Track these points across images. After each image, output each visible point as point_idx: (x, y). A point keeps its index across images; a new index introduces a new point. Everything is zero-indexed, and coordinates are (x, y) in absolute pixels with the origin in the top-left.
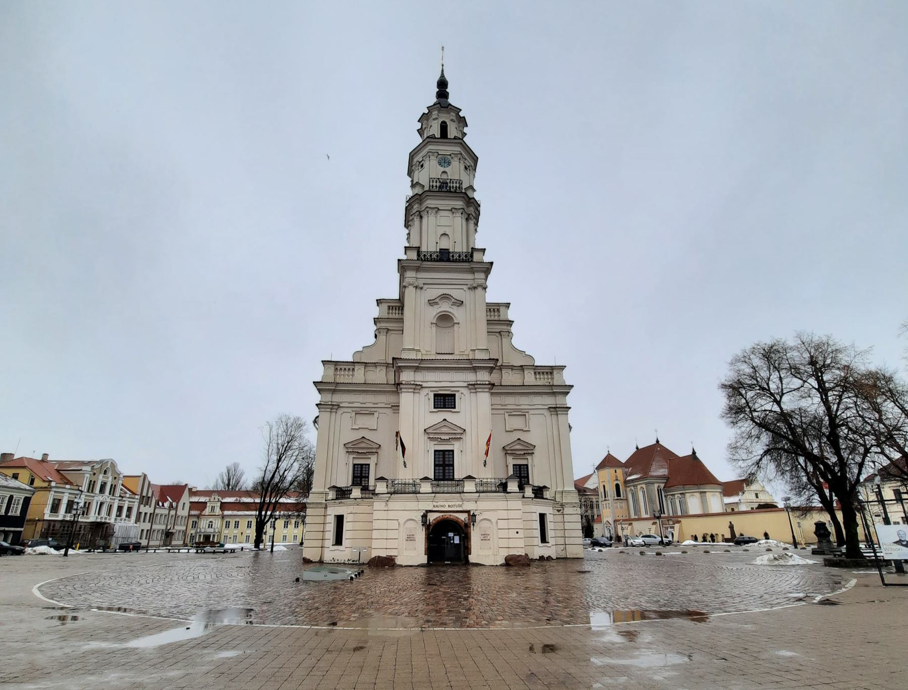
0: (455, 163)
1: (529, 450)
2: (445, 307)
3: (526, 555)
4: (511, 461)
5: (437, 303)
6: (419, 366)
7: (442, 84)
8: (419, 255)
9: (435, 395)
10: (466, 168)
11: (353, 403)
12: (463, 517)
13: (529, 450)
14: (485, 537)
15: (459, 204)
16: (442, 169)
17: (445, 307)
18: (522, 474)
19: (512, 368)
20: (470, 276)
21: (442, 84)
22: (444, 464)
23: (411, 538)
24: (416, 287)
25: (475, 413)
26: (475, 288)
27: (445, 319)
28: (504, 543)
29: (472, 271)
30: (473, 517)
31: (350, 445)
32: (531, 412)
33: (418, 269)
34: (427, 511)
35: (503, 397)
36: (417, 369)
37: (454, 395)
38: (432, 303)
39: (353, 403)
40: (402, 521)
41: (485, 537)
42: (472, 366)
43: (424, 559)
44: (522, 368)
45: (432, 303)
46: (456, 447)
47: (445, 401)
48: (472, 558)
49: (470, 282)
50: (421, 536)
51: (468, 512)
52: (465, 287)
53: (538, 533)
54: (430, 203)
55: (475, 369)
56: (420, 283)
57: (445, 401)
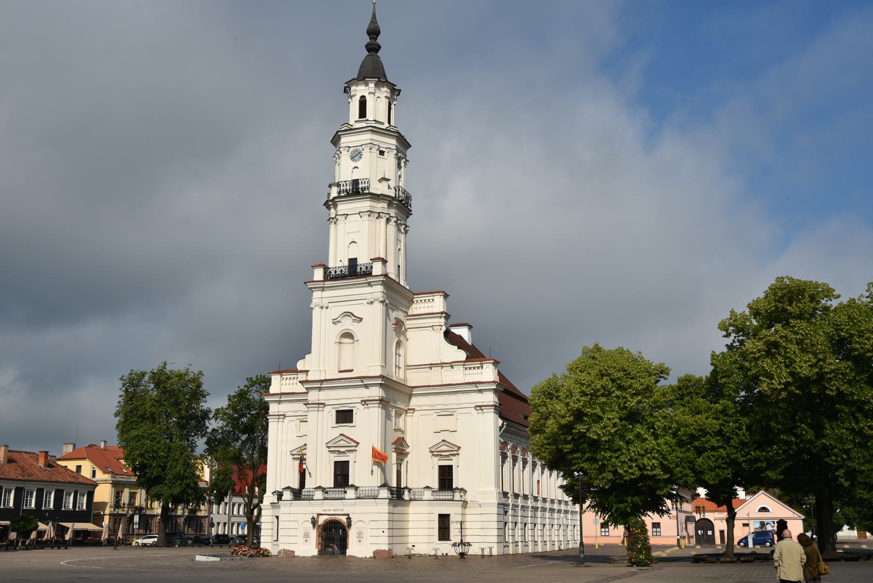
0: (366, 153)
1: (455, 450)
2: (348, 324)
3: (390, 550)
4: (438, 462)
5: (339, 322)
6: (322, 384)
7: (374, 33)
8: (325, 273)
9: (338, 412)
10: (382, 153)
11: (297, 411)
12: (344, 519)
13: (455, 450)
14: (360, 535)
15: (365, 204)
16: (354, 164)
17: (348, 324)
18: (446, 476)
19: (442, 365)
20: (368, 290)
21: (374, 33)
22: (342, 473)
23: (306, 535)
24: (322, 308)
25: (368, 426)
26: (372, 303)
27: (348, 335)
28: (374, 540)
29: (369, 284)
30: (349, 519)
31: (295, 452)
32: (459, 411)
33: (323, 289)
34: (319, 515)
35: (431, 397)
36: (320, 389)
37: (352, 411)
38: (335, 322)
39: (297, 411)
40: (300, 522)
41: (360, 535)
42: (364, 381)
43: (315, 552)
44: (452, 365)
45: (335, 322)
46: (349, 457)
47: (345, 416)
48: (349, 552)
49: (369, 296)
50: (314, 534)
51: (348, 515)
52: (365, 302)
53: (436, 532)
54: (342, 208)
55: (366, 386)
56: (325, 303)
57: (345, 416)
